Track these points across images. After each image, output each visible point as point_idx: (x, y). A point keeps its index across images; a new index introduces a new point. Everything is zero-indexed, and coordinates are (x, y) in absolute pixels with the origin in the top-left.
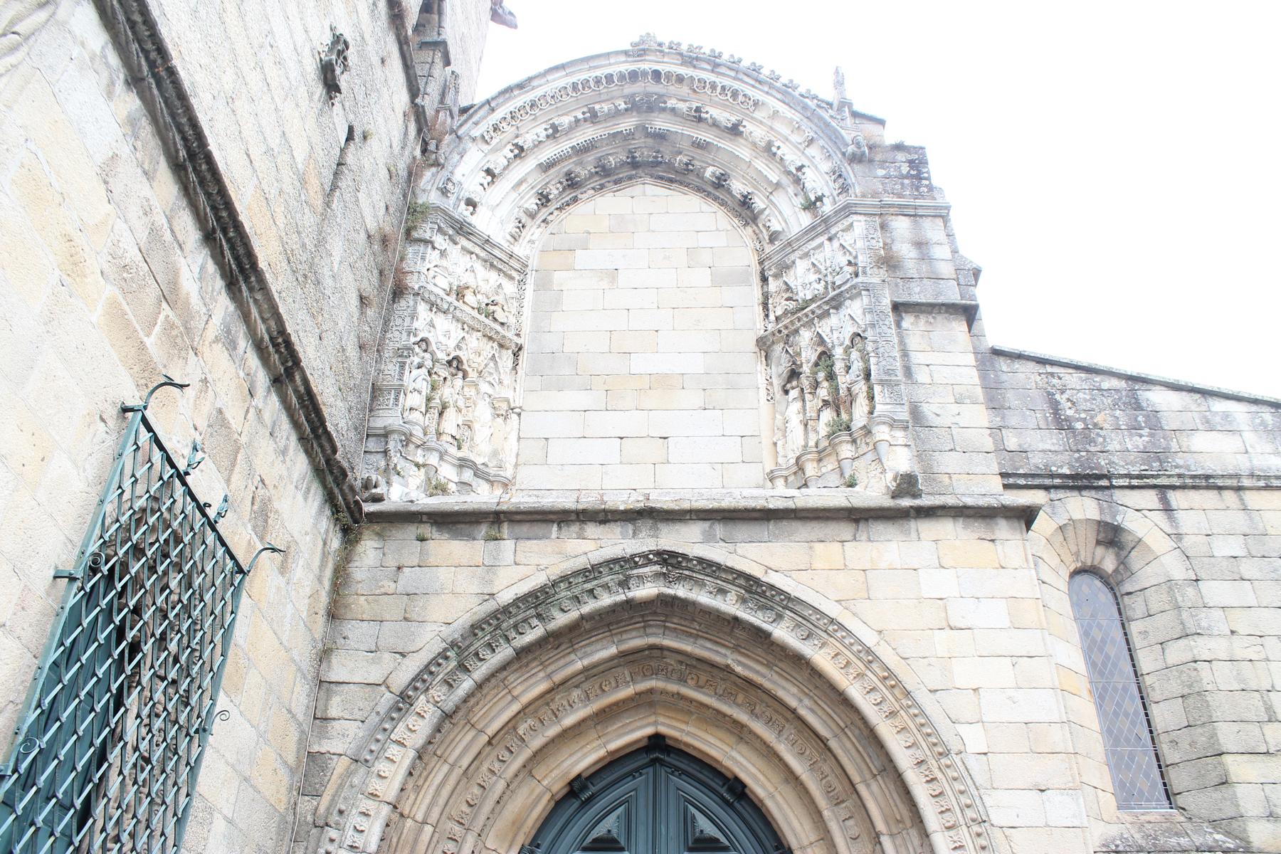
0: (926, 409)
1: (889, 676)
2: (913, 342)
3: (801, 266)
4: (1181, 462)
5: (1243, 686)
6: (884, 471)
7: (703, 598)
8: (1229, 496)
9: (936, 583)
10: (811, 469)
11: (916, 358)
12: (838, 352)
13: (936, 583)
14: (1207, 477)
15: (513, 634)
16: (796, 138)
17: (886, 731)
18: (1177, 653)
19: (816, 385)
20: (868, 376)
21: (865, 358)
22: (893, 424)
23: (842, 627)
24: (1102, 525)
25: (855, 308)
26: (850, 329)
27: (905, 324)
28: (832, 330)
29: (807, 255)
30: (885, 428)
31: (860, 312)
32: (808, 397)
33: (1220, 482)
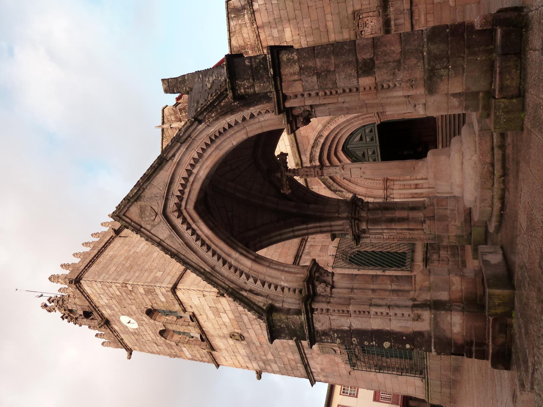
4: (254, 42)
5: (312, 34)
7: (318, 154)
14: (257, 37)
15: (331, 184)
33: (257, 33)
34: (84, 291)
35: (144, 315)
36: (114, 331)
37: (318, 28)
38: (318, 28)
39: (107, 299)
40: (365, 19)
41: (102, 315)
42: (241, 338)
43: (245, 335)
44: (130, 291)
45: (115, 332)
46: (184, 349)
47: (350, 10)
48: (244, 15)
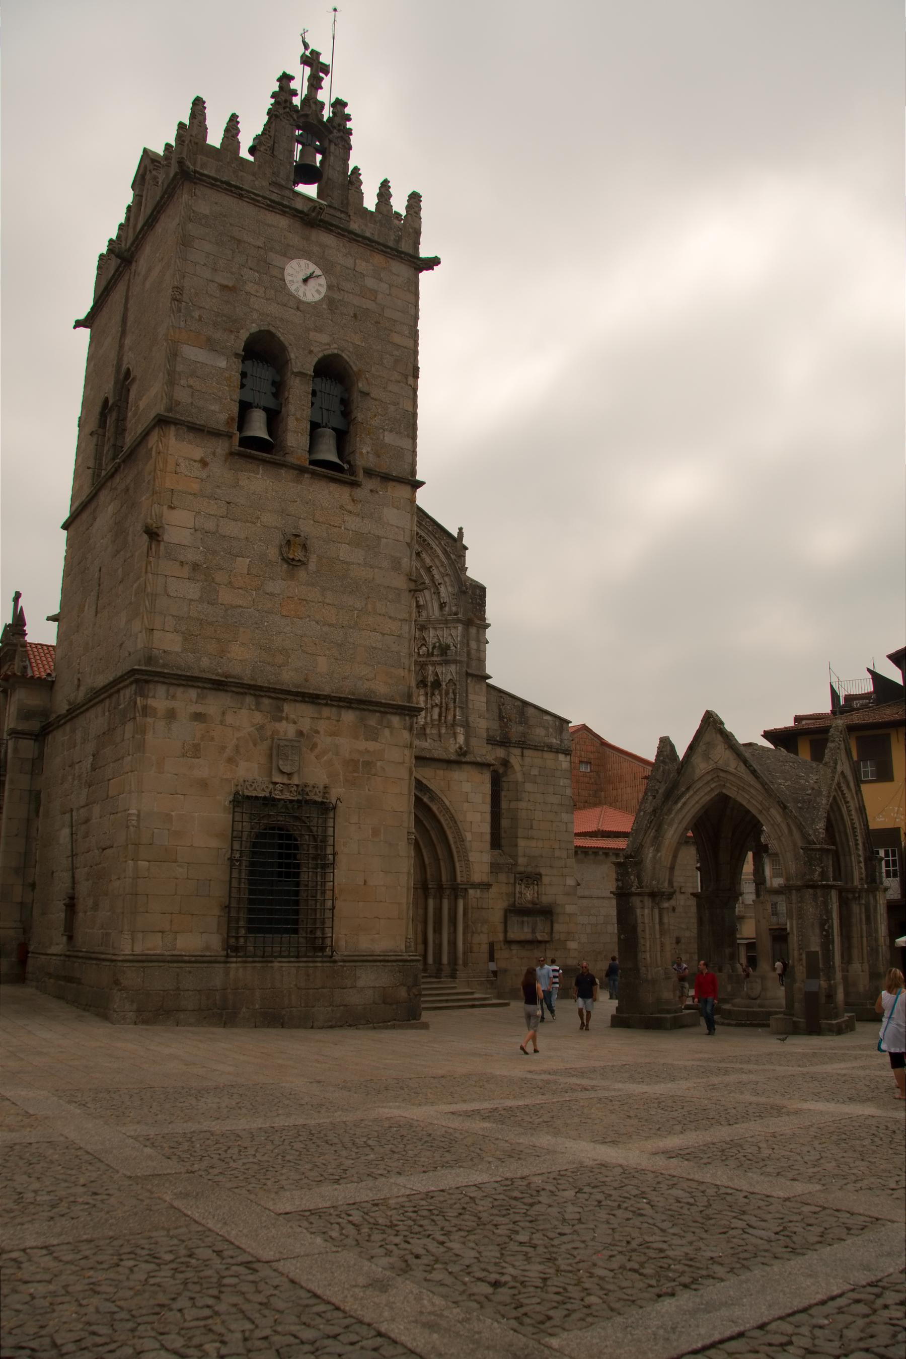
0: (471, 719)
1: (452, 818)
2: (470, 690)
3: (432, 633)
6: (456, 743)
8: (539, 754)
9: (467, 787)
10: (428, 731)
11: (471, 697)
12: (444, 684)
13: (467, 787)
14: (535, 746)
16: (442, 569)
17: (448, 832)
18: (513, 805)
19: (433, 694)
20: (455, 702)
21: (454, 694)
22: (462, 726)
23: (442, 800)
24: (504, 759)
25: (453, 668)
26: (449, 677)
27: (469, 681)
28: (442, 673)
29: (435, 629)
30: (459, 728)
31: (455, 671)
32: (429, 698)
34: (402, 258)
35: (335, 346)
36: (273, 207)
37: (532, 828)
38: (532, 828)
39: (376, 292)
40: (532, 887)
41: (326, 228)
42: (299, 561)
43: (302, 574)
44: (406, 377)
45: (268, 205)
46: (222, 364)
47: (543, 871)
48: (556, 738)
